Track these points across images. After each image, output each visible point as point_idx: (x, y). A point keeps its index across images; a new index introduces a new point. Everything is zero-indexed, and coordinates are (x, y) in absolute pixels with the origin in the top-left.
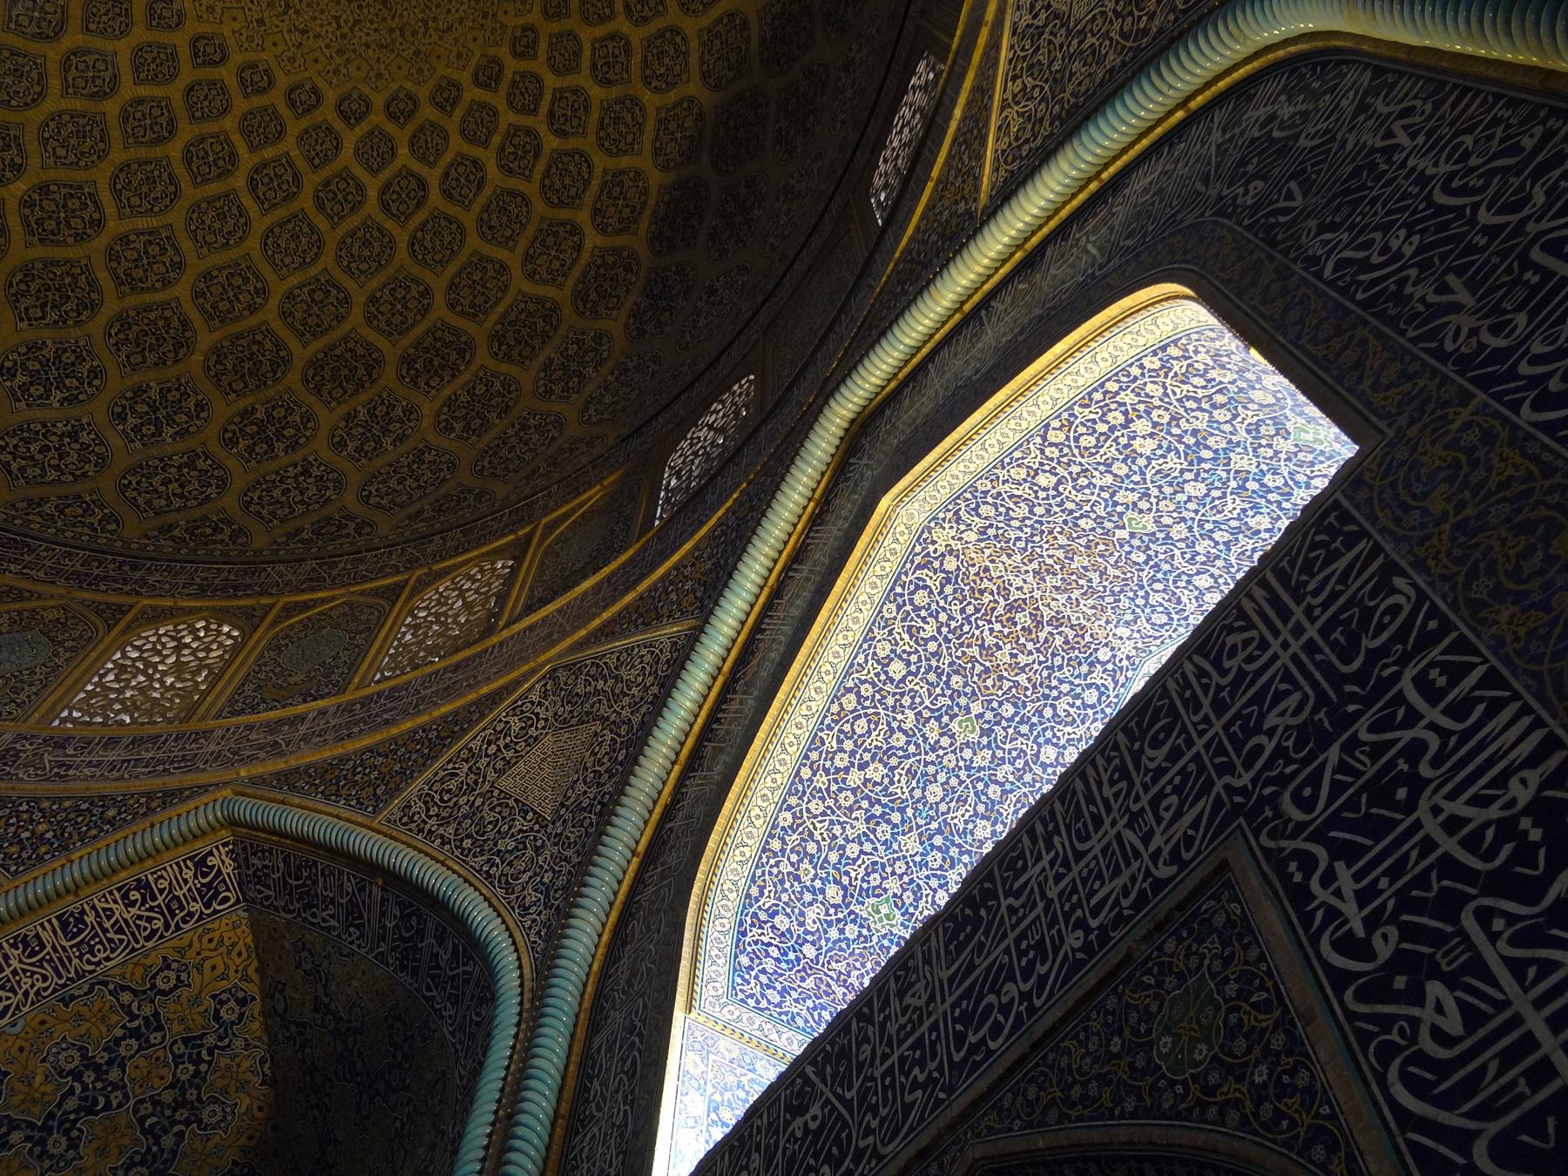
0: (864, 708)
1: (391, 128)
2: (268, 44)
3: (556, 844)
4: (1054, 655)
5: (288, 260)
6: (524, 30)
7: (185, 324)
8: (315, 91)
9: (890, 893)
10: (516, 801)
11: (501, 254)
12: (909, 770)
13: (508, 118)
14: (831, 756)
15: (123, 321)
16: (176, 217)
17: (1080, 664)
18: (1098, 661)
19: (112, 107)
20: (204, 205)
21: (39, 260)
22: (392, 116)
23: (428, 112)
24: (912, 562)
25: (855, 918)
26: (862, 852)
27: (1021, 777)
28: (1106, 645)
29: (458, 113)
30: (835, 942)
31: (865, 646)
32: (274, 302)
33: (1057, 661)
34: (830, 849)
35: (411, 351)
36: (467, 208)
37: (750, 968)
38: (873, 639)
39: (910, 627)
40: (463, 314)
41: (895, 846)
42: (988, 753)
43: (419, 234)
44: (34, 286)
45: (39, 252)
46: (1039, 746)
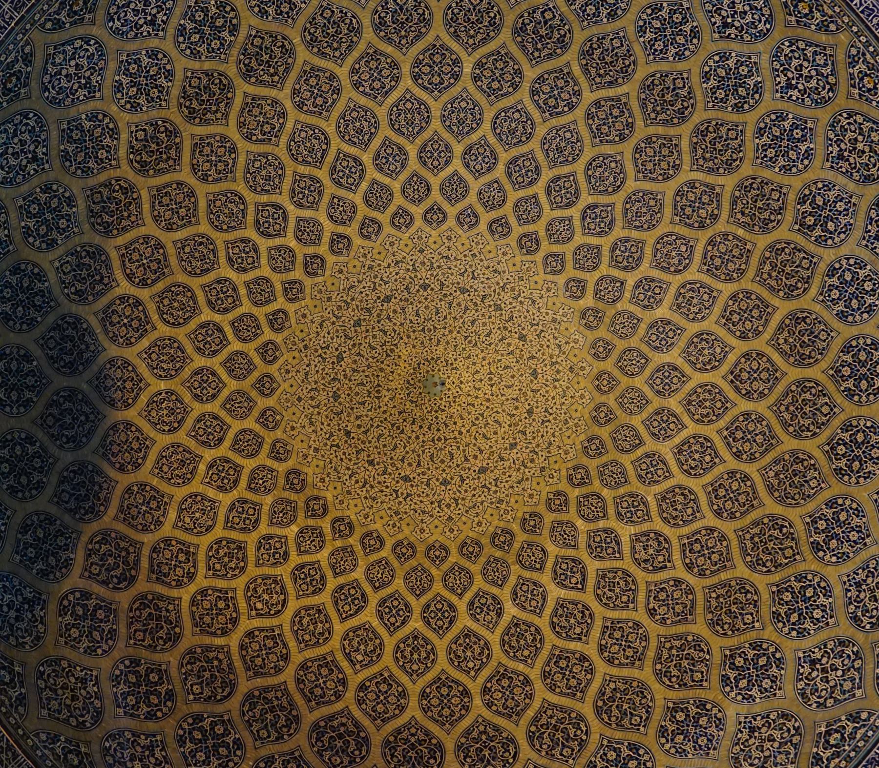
1: (311, 250)
2: (410, 242)
5: (303, 135)
6: (276, 359)
7: (324, 55)
8: (367, 237)
11: (180, 235)
13: (246, 307)
15: (357, 31)
16: (382, 112)
19: (458, 149)
20: (373, 130)
21: (426, 34)
22: (316, 256)
23: (298, 273)
29: (278, 287)
32: (288, 104)
35: (177, 140)
36: (227, 243)
40: (168, 185)
43: (242, 207)
44: (416, 17)
45: (430, 38)
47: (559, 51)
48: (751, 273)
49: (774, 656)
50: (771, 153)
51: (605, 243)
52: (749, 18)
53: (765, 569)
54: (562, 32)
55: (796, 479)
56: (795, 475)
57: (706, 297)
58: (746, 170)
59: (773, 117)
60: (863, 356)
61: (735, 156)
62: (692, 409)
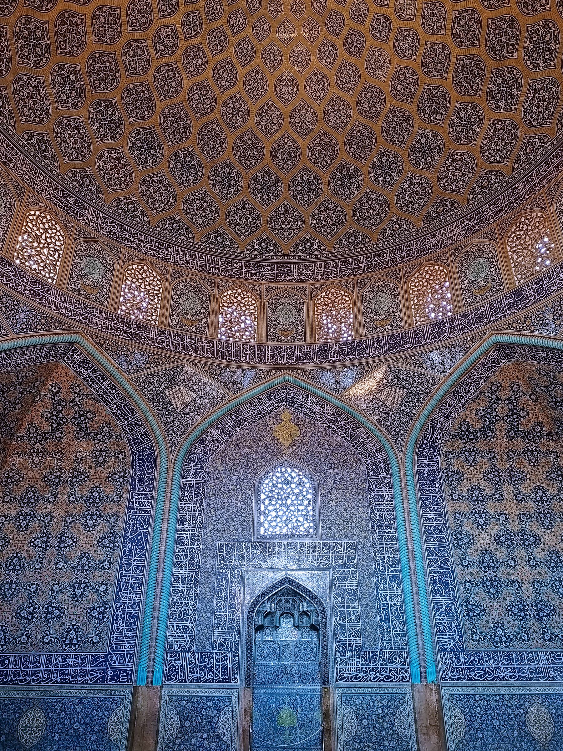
47: (488, 44)
48: (326, 128)
49: (117, 133)
50: (384, 159)
51: (365, 29)
52: (450, 176)
53: (162, 122)
54: (497, 53)
55: (211, 142)
56: (214, 142)
57: (318, 94)
58: (381, 140)
59: (401, 168)
60: (273, 188)
61: (389, 136)
62: (253, 74)
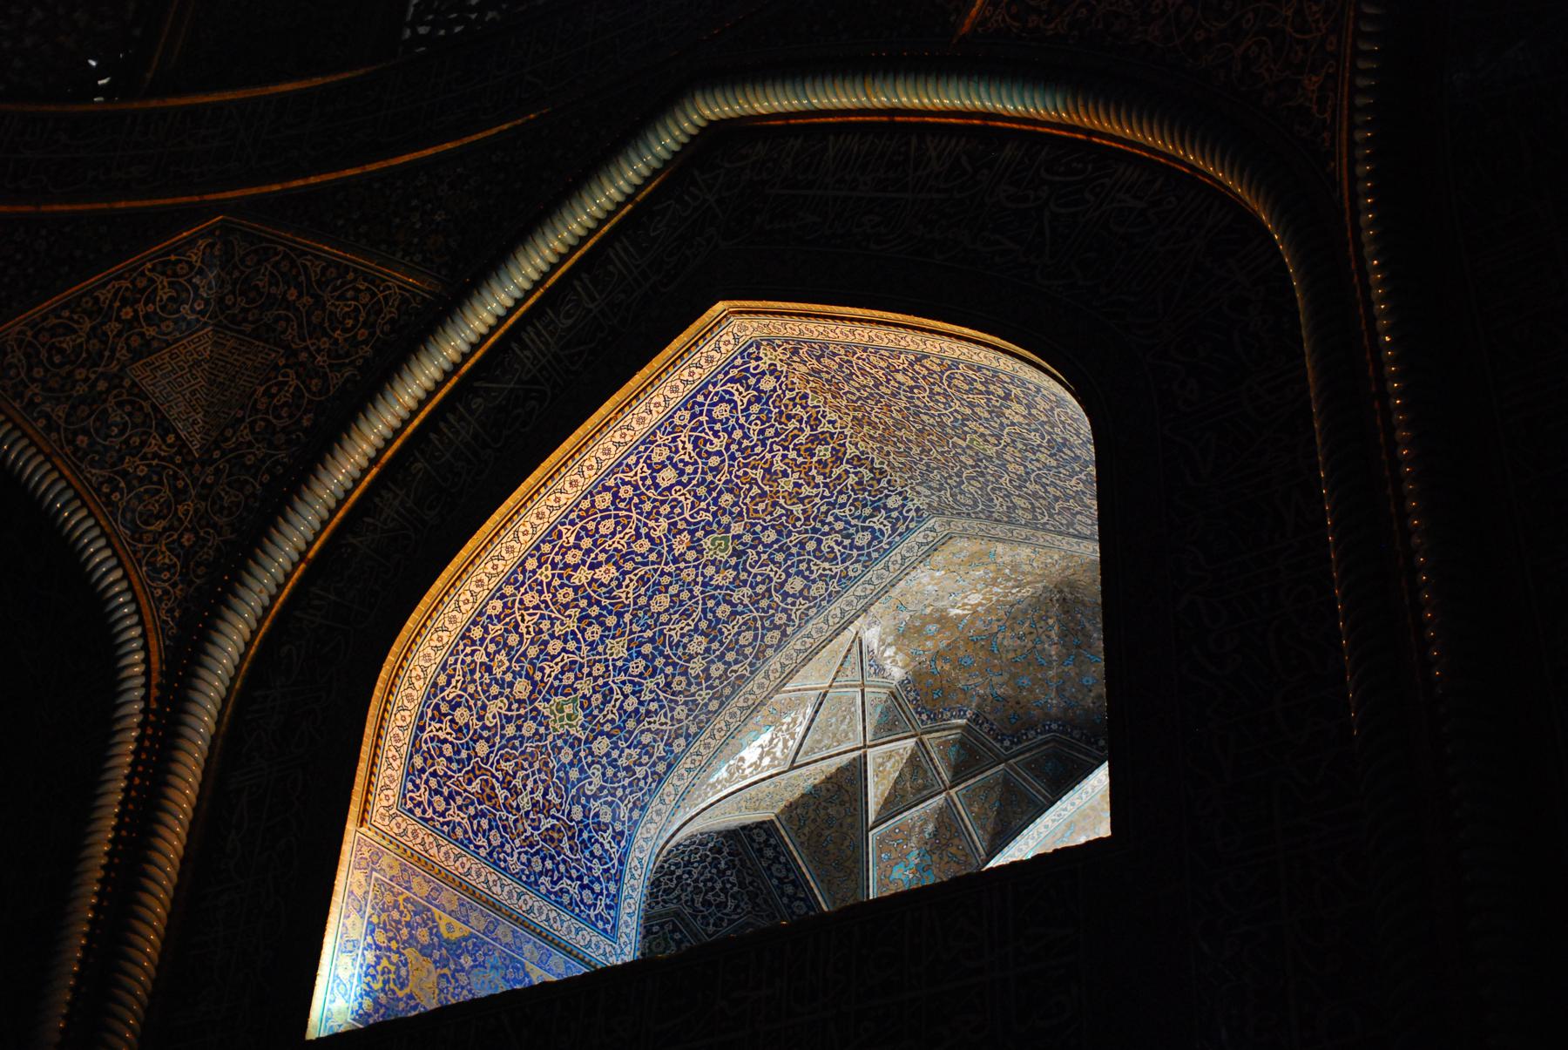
0: (617, 509)
3: (204, 498)
4: (841, 492)
9: (580, 694)
10: (153, 406)
12: (642, 578)
14: (564, 551)
17: (865, 506)
18: (885, 507)
24: (726, 373)
25: (536, 715)
26: (564, 650)
27: (757, 602)
28: (900, 494)
30: (509, 739)
31: (642, 448)
33: (842, 499)
34: (532, 643)
37: (423, 770)
38: (652, 443)
39: (698, 438)
41: (600, 648)
42: (731, 574)
46: (789, 575)
